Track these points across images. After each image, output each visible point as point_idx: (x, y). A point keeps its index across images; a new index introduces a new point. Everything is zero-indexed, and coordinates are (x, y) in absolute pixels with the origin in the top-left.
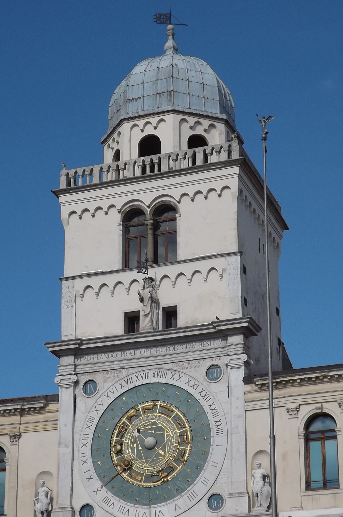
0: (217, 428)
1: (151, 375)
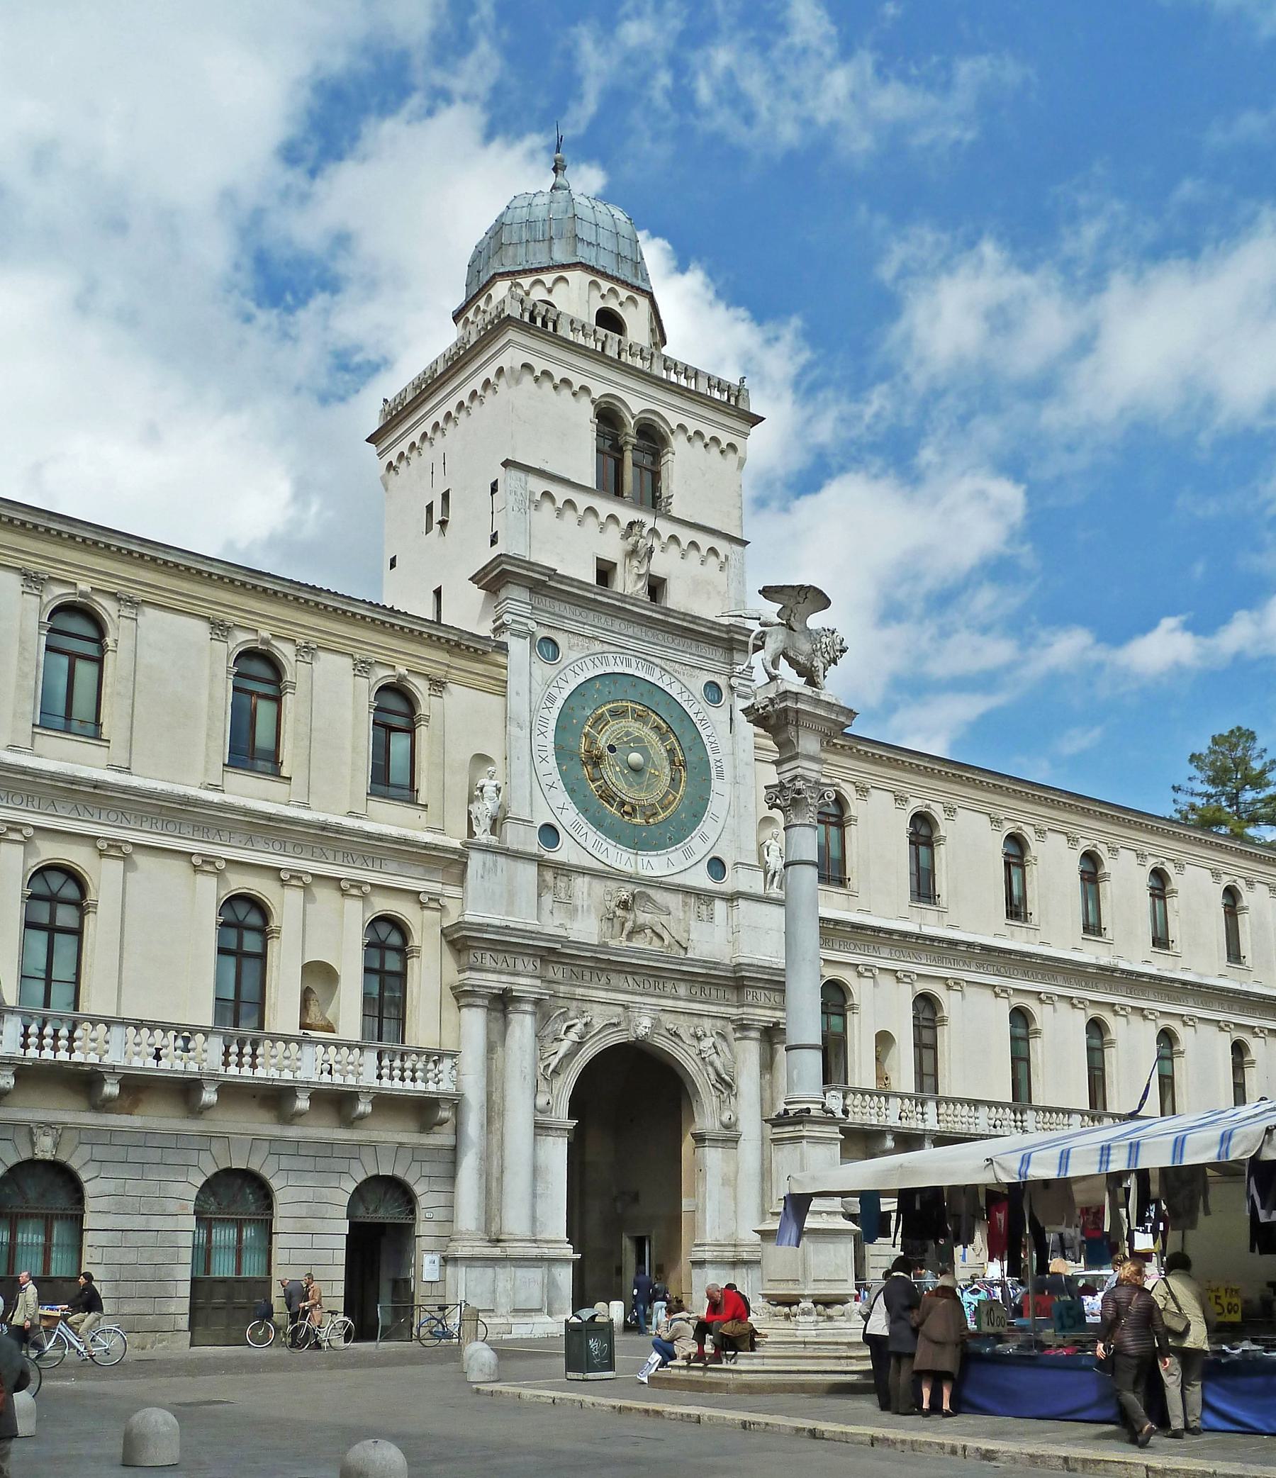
1: (634, 665)
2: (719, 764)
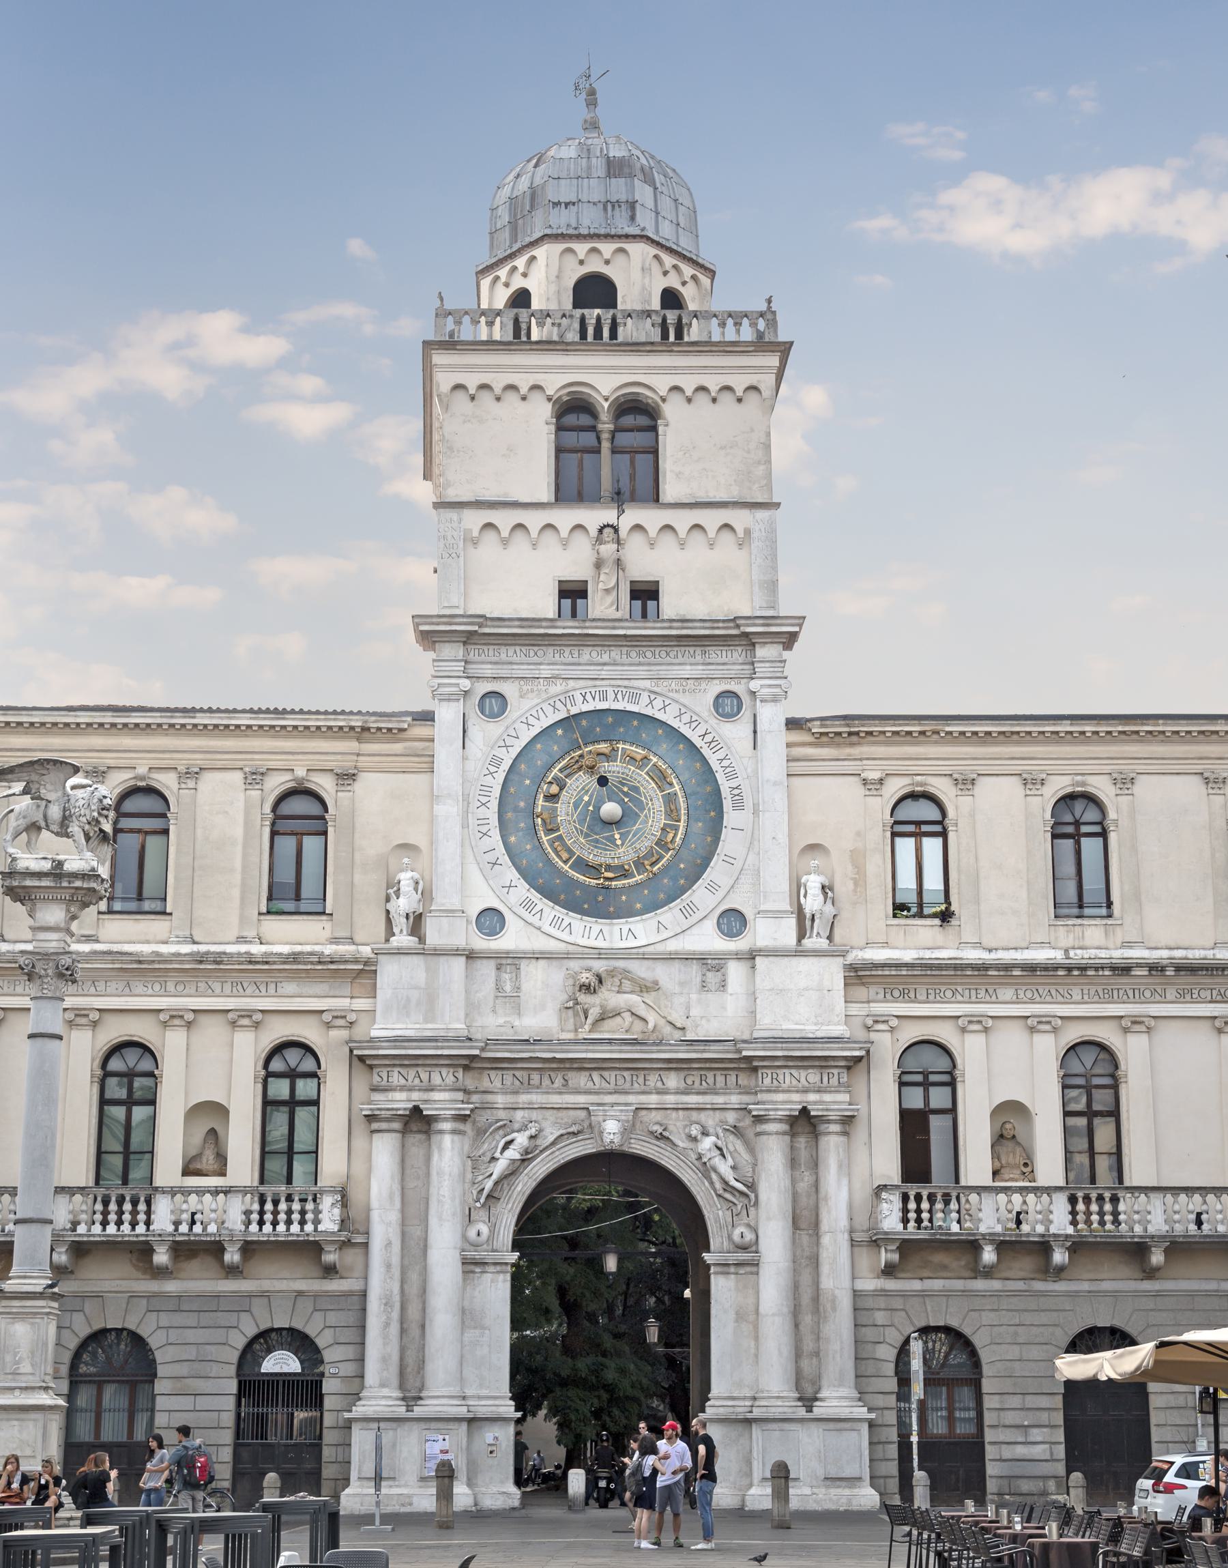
1: (611, 695)
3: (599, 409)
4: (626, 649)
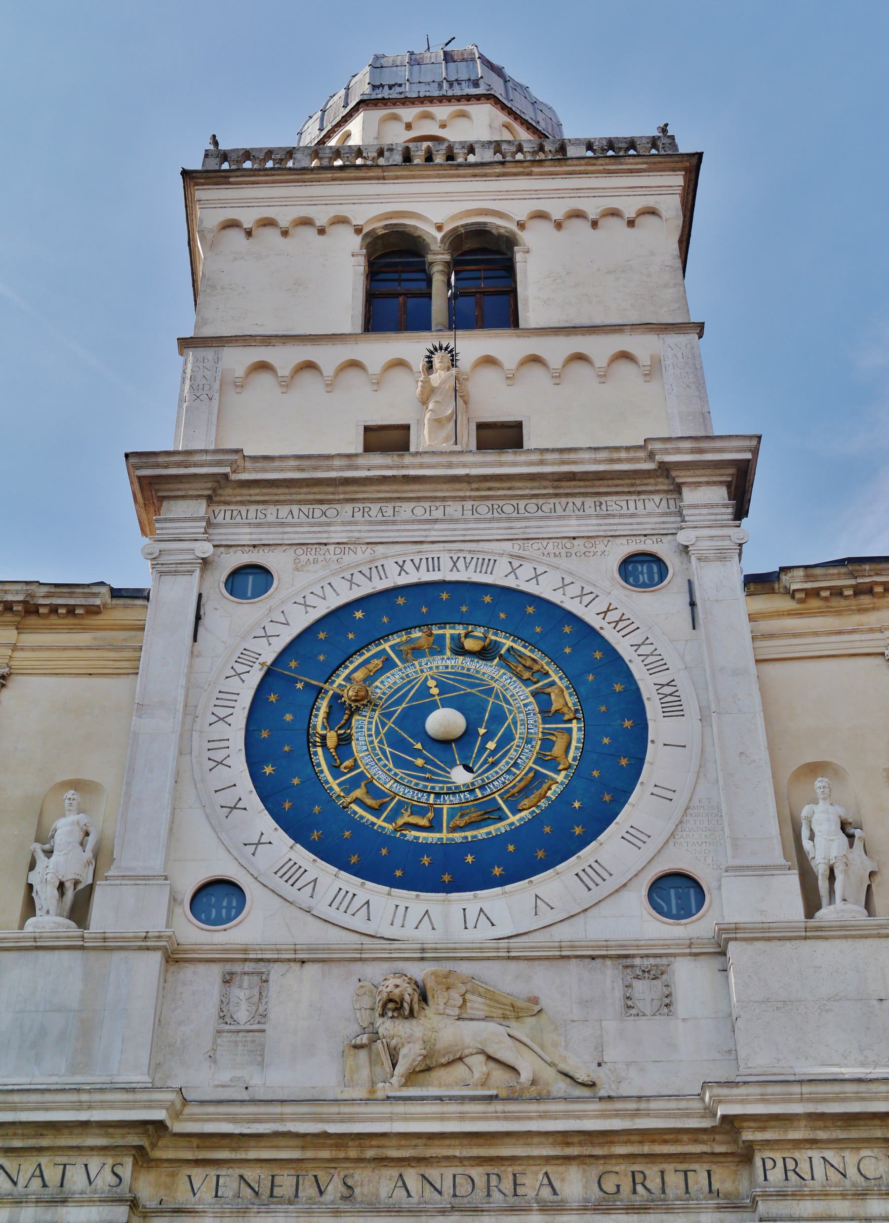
0: (662, 701)
1: (446, 563)
2: (667, 690)
3: (428, 240)
4: (472, 503)
